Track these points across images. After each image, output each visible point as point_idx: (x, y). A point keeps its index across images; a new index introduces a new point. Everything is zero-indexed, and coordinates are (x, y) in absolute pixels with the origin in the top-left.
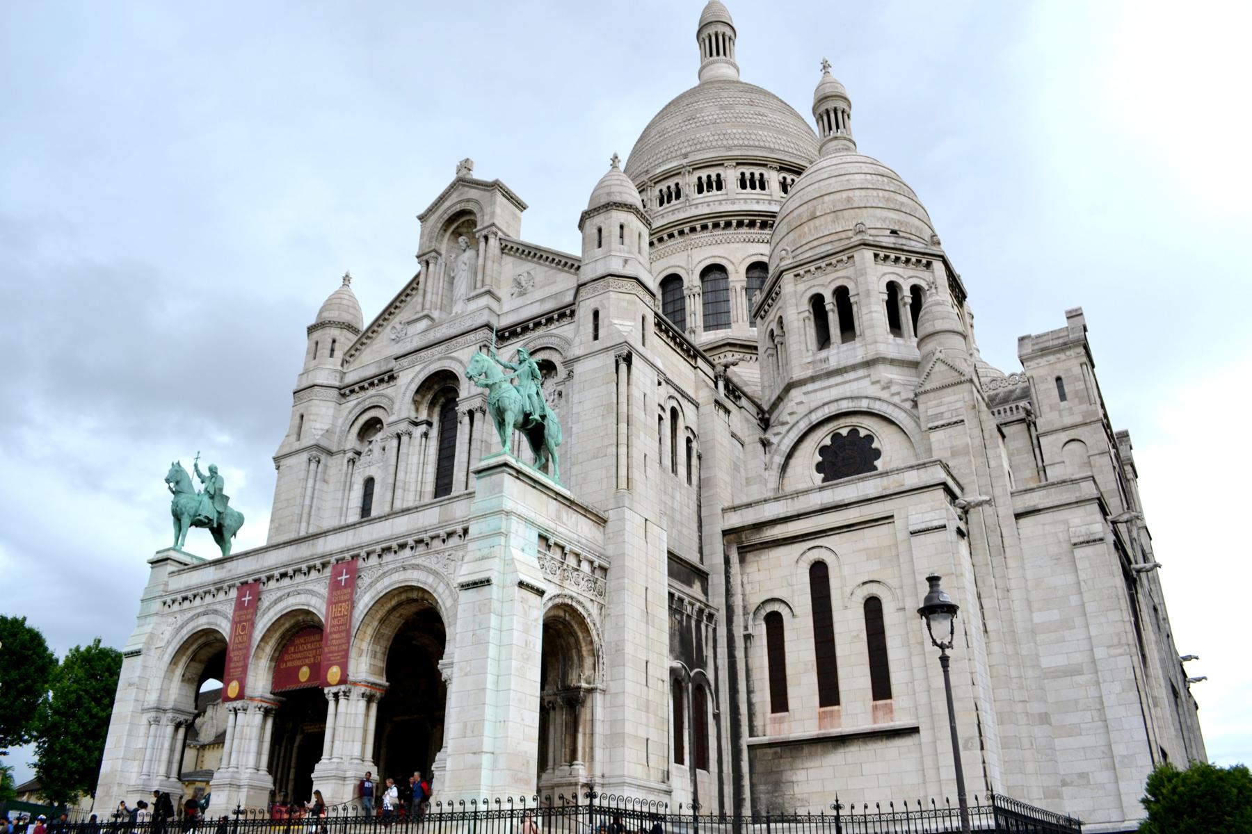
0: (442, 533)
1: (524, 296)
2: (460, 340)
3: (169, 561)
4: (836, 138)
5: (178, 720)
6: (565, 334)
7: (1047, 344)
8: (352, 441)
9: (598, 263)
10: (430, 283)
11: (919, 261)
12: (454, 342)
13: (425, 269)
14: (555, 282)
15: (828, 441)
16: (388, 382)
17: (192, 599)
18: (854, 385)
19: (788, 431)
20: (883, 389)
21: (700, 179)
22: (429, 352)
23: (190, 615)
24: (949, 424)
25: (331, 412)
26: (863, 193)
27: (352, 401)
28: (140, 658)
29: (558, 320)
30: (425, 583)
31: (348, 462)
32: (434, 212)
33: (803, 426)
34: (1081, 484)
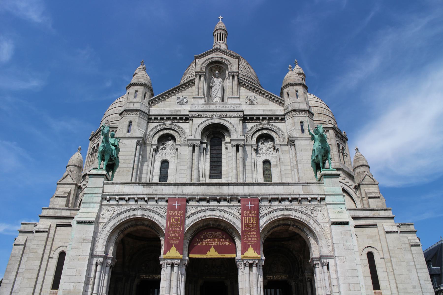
0: (309, 197)
1: (253, 105)
3: (105, 176)
5: (111, 265)
6: (279, 126)
8: (155, 141)
9: (300, 104)
11: (343, 139)
12: (225, 114)
13: (198, 78)
14: (268, 104)
16: (178, 120)
17: (128, 200)
20: (343, 179)
22: (211, 114)
23: (126, 208)
24: (375, 197)
25: (145, 124)
26: (326, 110)
28: (92, 226)
29: (274, 120)
30: (301, 218)
31: (153, 150)
32: (203, 57)
34: (410, 226)
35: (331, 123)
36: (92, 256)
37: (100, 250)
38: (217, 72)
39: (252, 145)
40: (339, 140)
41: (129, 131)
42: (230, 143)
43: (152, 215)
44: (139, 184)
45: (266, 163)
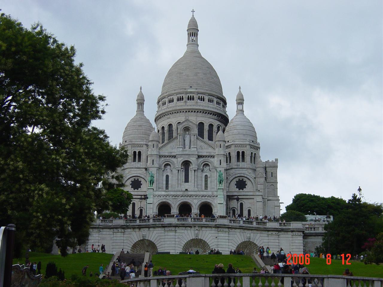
0: (213, 196)
2: (192, 156)
4: (241, 111)
7: (271, 165)
8: (163, 167)
9: (221, 151)
10: (181, 140)
14: (209, 149)
15: (238, 180)
18: (244, 171)
19: (231, 177)
21: (199, 96)
22: (185, 156)
27: (163, 159)
28: (152, 204)
33: (234, 177)
35: (249, 142)
36: (153, 213)
37: (155, 211)
38: (187, 132)
39: (201, 169)
40: (253, 150)
41: (153, 164)
42: (192, 168)
43: (168, 201)
44: (163, 191)
45: (206, 176)
